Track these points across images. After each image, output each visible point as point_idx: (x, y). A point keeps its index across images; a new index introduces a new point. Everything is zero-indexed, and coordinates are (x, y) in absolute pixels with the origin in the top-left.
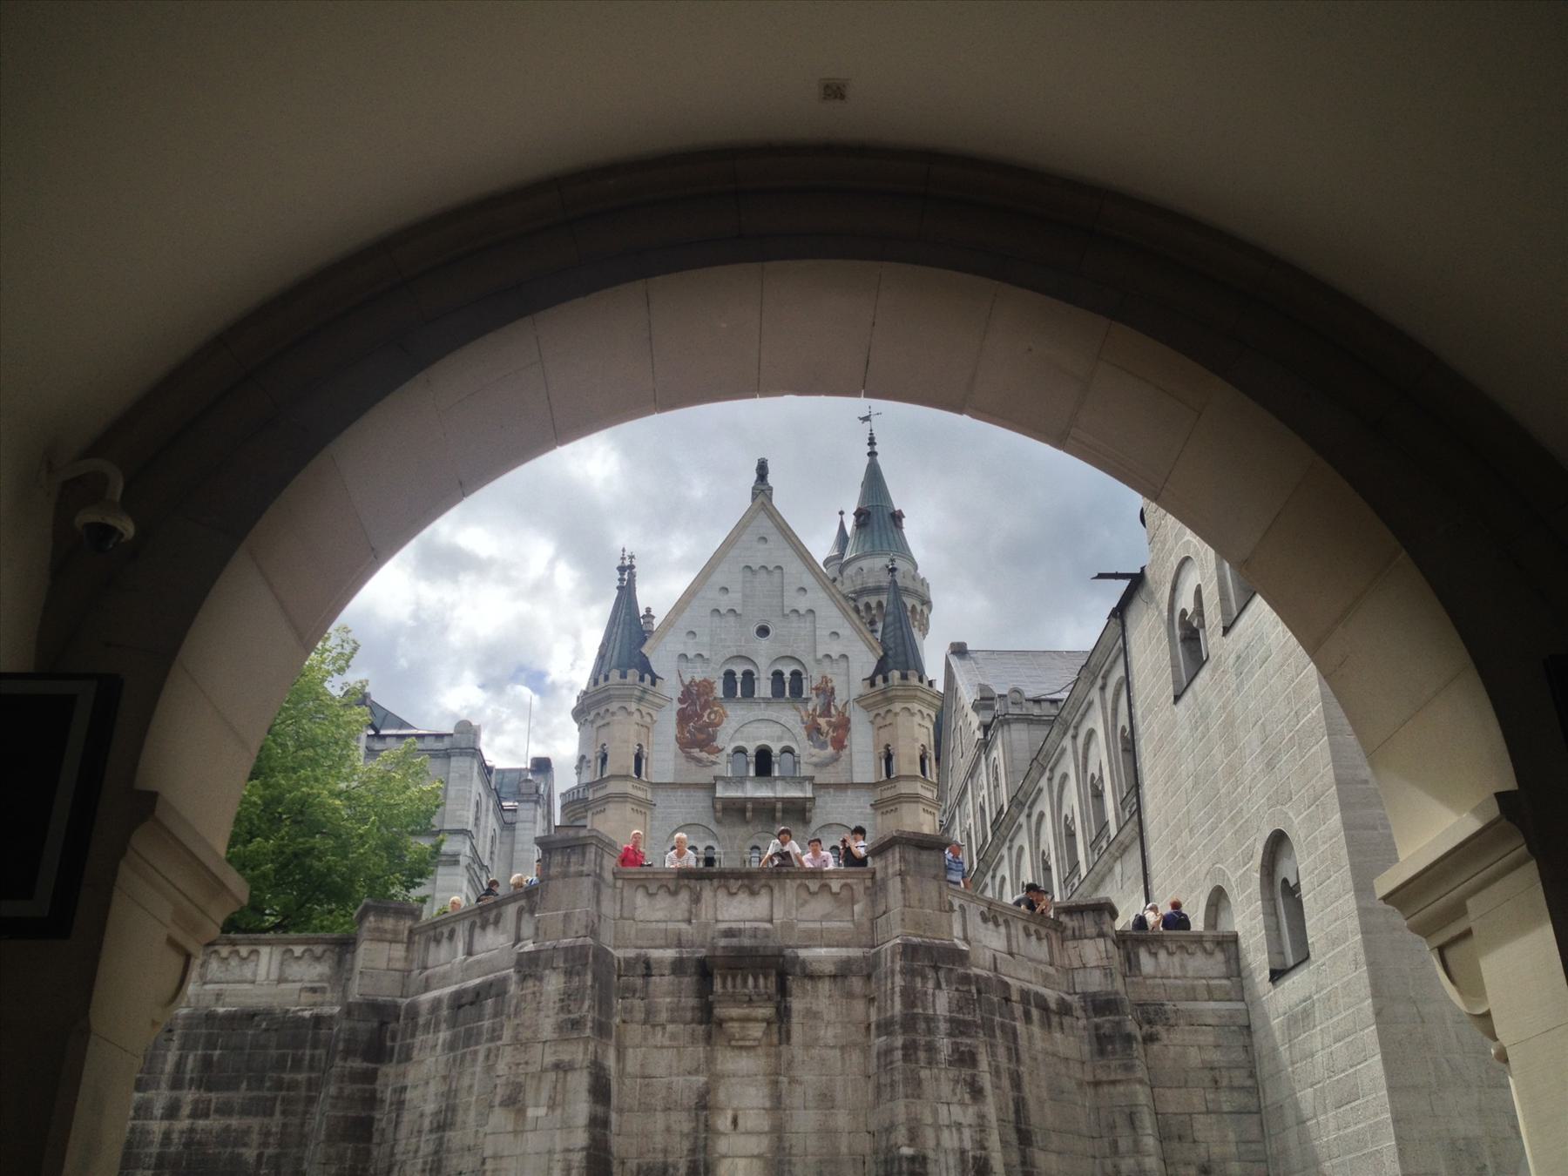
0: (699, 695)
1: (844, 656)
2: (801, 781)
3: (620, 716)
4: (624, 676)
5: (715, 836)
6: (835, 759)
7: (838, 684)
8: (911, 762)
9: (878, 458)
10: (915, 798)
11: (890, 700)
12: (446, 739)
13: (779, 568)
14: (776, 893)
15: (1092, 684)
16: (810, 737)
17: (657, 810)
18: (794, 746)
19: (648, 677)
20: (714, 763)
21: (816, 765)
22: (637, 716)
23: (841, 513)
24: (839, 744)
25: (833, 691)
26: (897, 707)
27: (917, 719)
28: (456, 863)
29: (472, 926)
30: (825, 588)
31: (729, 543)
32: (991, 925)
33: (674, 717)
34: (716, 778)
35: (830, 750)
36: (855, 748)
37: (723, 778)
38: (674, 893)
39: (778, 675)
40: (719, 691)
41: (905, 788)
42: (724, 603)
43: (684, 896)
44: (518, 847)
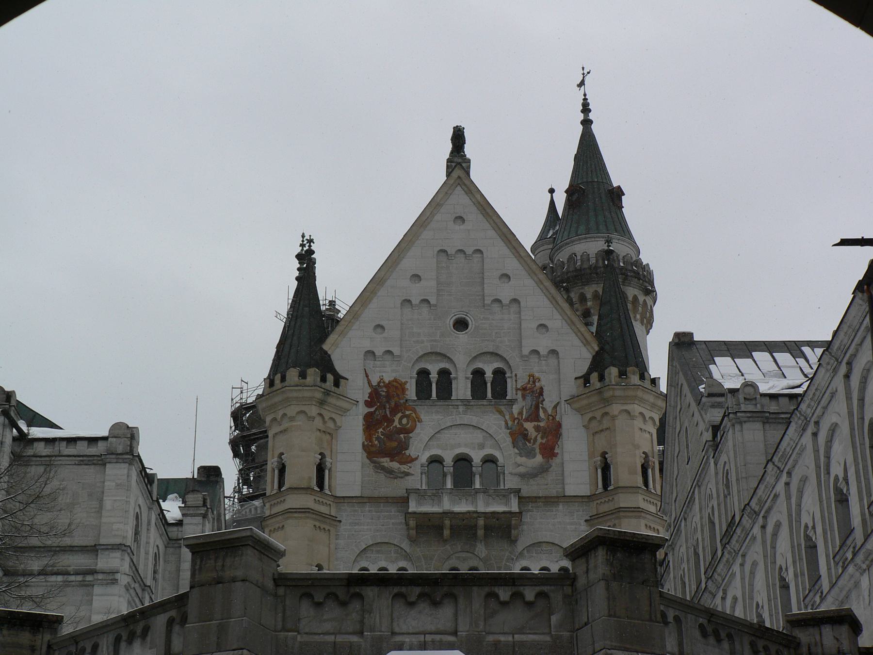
0: (389, 397)
1: (554, 352)
2: (505, 495)
3: (300, 421)
4: (303, 375)
5: (407, 557)
6: (543, 470)
7: (546, 382)
10: (637, 511)
11: (607, 402)
12: (101, 444)
13: (479, 251)
14: (461, 601)
15: (835, 371)
16: (515, 444)
17: (342, 527)
18: (497, 454)
19: (330, 377)
20: (408, 474)
21: (522, 476)
22: (318, 420)
23: (552, 191)
24: (549, 452)
25: (542, 388)
27: (638, 423)
28: (114, 582)
29: (118, 640)
30: (531, 273)
32: (712, 640)
35: (539, 459)
36: (566, 457)
37: (417, 491)
38: (344, 604)
39: (478, 374)
40: (411, 392)
42: (416, 292)
43: (356, 605)
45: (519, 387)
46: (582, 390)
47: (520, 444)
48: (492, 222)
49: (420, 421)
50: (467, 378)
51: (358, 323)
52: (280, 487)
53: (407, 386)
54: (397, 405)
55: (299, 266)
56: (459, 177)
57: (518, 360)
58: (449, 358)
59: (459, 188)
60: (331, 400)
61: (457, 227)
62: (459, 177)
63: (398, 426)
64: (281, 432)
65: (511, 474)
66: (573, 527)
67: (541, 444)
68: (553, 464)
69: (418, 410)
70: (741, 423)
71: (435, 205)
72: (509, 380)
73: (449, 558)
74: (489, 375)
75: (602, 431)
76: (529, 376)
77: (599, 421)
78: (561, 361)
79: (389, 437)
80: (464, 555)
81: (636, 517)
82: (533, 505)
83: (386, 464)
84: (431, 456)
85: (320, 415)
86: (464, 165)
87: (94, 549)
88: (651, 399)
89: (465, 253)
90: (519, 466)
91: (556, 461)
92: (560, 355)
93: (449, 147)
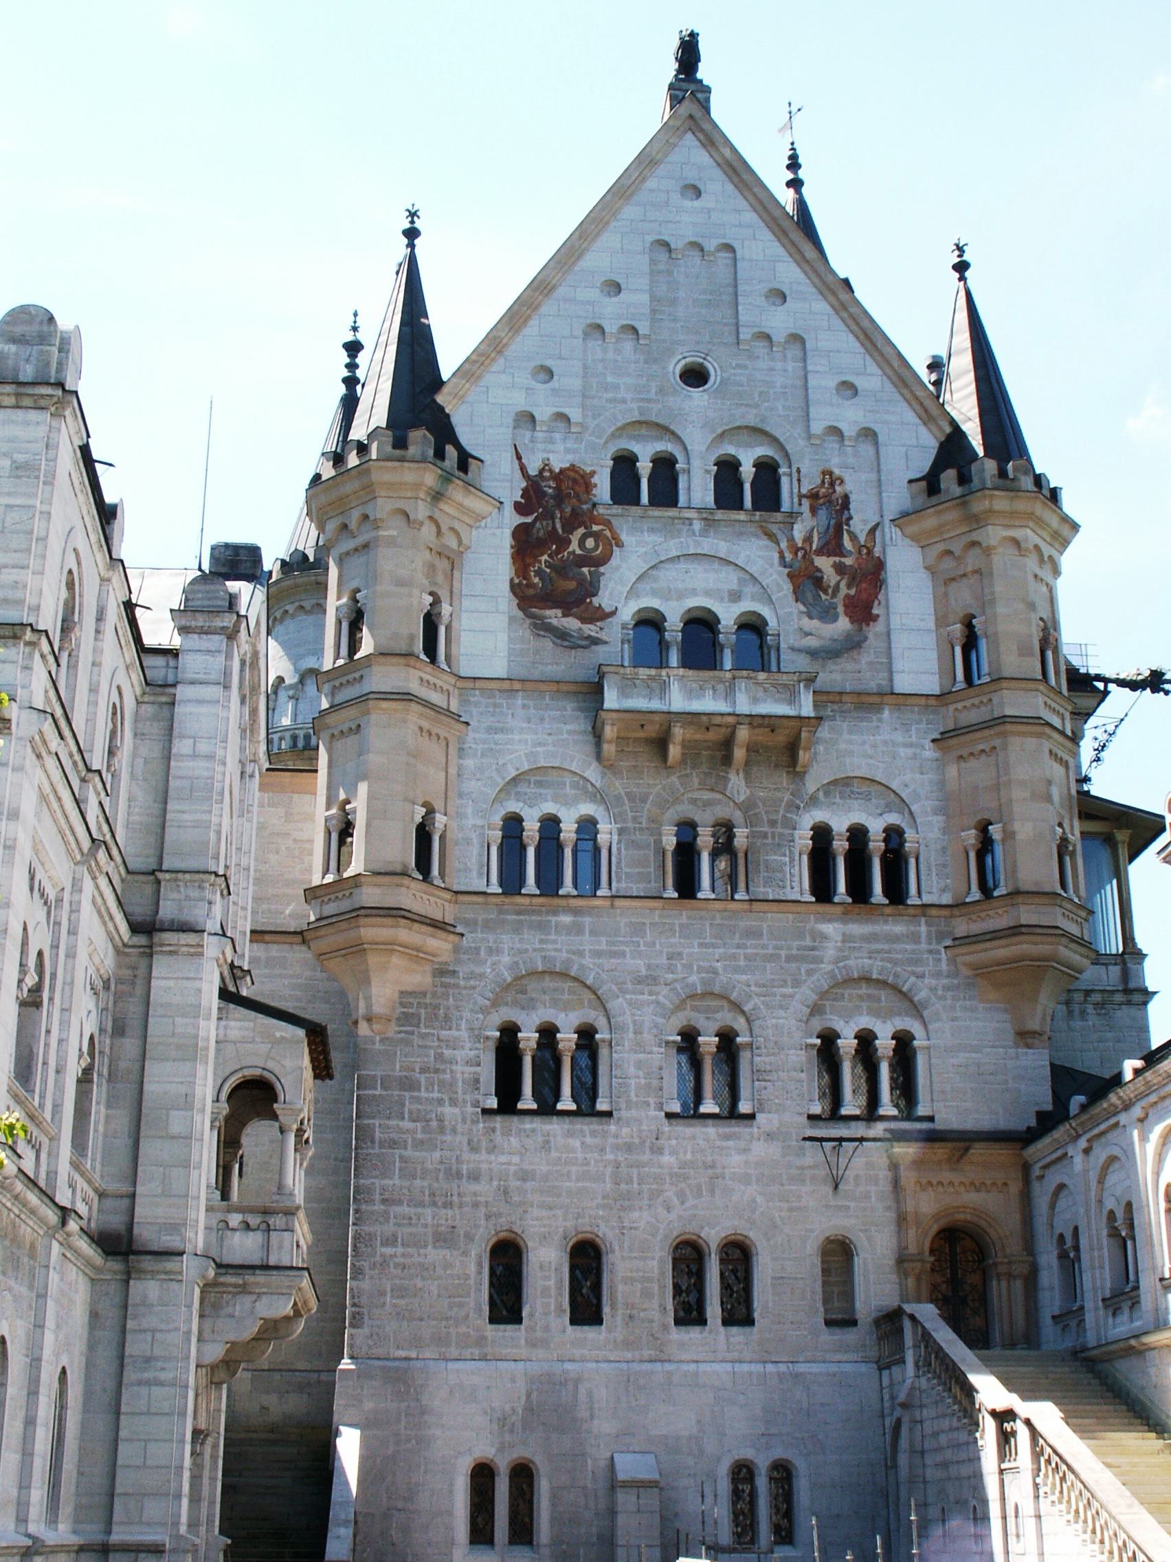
0: (560, 497)
1: (869, 434)
4: (400, 443)
5: (598, 796)
6: (852, 644)
7: (855, 485)
8: (1024, 651)
9: (804, 190)
11: (976, 521)
13: (729, 248)
16: (798, 596)
18: (766, 612)
20: (595, 641)
21: (813, 653)
22: (428, 531)
24: (863, 611)
26: (994, 534)
27: (1031, 563)
31: (622, 191)
33: (505, 542)
35: (843, 624)
36: (895, 622)
41: (1014, 703)
42: (612, 312)
44: (181, 747)
45: (804, 491)
46: (922, 499)
47: (809, 595)
48: (750, 198)
49: (620, 544)
50: (708, 472)
51: (501, 361)
53: (595, 480)
54: (575, 513)
55: (348, 360)
56: (691, 117)
57: (802, 443)
58: (673, 433)
59: (689, 135)
61: (688, 204)
62: (691, 117)
63: (579, 552)
64: (356, 550)
65: (793, 649)
66: (910, 751)
67: (847, 596)
68: (871, 636)
69: (614, 522)
71: (646, 161)
72: (785, 481)
73: (677, 801)
74: (747, 471)
75: (964, 575)
76: (824, 473)
77: (958, 559)
78: (882, 450)
79: (561, 570)
80: (707, 795)
81: (1032, 735)
82: (836, 707)
83: (554, 622)
84: (640, 611)
85: (430, 518)
86: (699, 95)
88: (1054, 522)
89: (702, 250)
90: (807, 634)
92: (881, 439)
93: (669, 69)
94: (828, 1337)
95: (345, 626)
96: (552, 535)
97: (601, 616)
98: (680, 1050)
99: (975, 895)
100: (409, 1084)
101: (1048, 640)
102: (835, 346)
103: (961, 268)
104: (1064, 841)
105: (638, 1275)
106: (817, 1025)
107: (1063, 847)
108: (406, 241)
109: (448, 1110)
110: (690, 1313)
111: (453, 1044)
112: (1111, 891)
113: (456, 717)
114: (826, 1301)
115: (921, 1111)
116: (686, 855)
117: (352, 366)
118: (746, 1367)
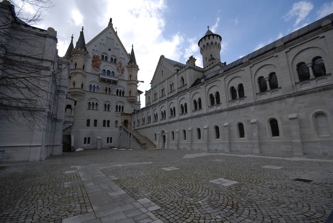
0: (97, 58)
1: (124, 58)
3: (80, 57)
4: (81, 49)
5: (99, 84)
6: (121, 75)
7: (123, 62)
11: (132, 67)
12: (44, 31)
13: (113, 39)
16: (117, 70)
22: (84, 58)
24: (122, 73)
26: (133, 69)
34: (100, 74)
35: (121, 73)
37: (101, 74)
39: (112, 58)
40: (101, 58)
45: (119, 62)
52: (75, 68)
60: (86, 55)
70: (190, 69)
72: (117, 61)
87: (42, 60)
91: (123, 75)
93: (109, 21)
94: (115, 128)
95: (75, 65)
96: (96, 61)
97: (100, 69)
98: (105, 105)
99: (129, 96)
100: (80, 106)
101: (136, 78)
102: (121, 49)
103: (133, 46)
104: (136, 93)
105: (100, 123)
106: (116, 104)
107: (136, 93)
108: (82, 30)
109: (83, 109)
110: (104, 126)
111: (84, 103)
112: (139, 96)
113: (86, 75)
114: (116, 125)
115: (124, 111)
116: (106, 90)
117: (72, 39)
118: (108, 130)
